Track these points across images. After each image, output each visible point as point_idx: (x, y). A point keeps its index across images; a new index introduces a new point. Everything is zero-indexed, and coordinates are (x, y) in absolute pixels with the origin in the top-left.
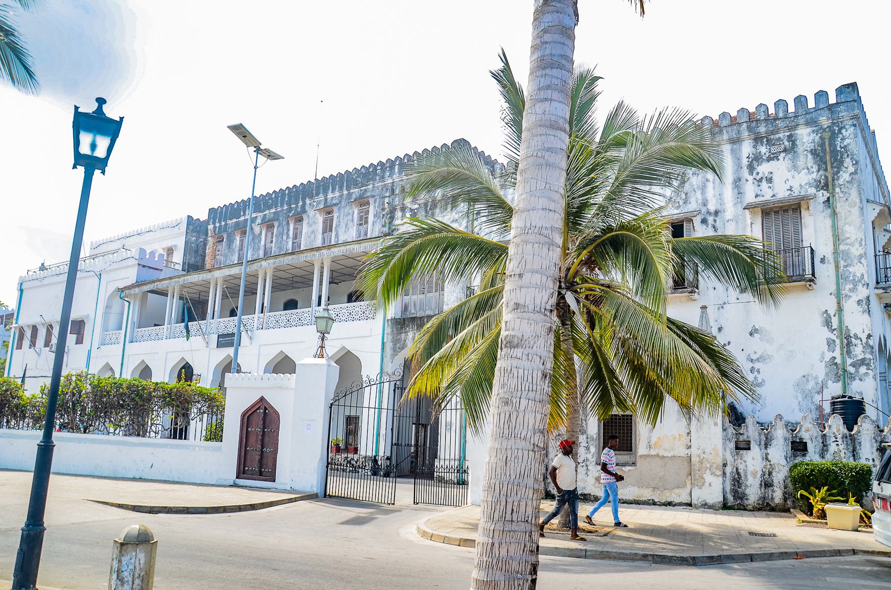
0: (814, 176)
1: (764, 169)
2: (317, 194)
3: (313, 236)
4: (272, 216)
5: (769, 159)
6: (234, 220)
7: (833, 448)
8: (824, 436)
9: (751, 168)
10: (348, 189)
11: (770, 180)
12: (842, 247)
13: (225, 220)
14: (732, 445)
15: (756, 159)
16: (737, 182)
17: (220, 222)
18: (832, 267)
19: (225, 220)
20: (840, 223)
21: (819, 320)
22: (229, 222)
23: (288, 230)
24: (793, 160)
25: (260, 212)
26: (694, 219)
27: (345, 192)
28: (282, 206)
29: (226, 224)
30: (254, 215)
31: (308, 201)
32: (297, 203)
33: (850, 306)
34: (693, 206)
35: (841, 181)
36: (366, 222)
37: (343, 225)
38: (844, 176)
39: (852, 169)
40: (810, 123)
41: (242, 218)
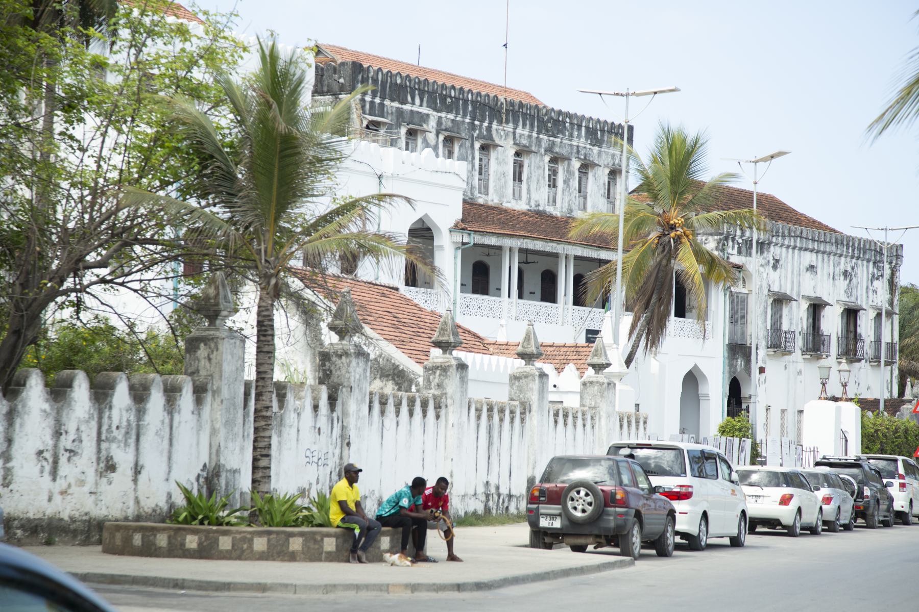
2: (507, 122)
3: (503, 180)
4: (450, 124)
6: (396, 104)
10: (539, 133)
13: (383, 98)
17: (374, 95)
19: (383, 98)
22: (387, 102)
23: (473, 158)
25: (435, 109)
27: (535, 135)
28: (464, 116)
29: (382, 105)
30: (424, 110)
31: (495, 125)
32: (482, 121)
36: (555, 186)
37: (534, 179)
41: (407, 107)
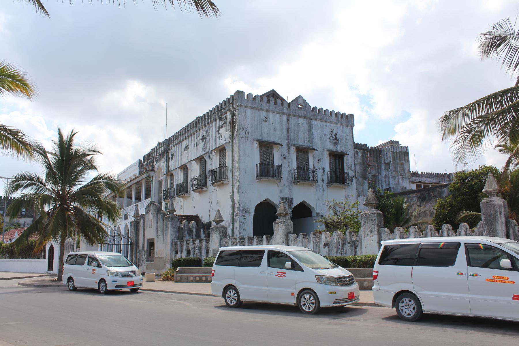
0: (230, 133)
1: (220, 131)
5: (222, 127)
7: (196, 252)
8: (194, 247)
9: (218, 132)
11: (221, 136)
12: (234, 164)
14: (174, 252)
15: (220, 127)
16: (216, 137)
18: (231, 173)
20: (234, 154)
21: (229, 197)
24: (226, 127)
26: (204, 156)
33: (235, 190)
34: (207, 150)
35: (235, 135)
38: (235, 132)
39: (237, 130)
40: (229, 110)
